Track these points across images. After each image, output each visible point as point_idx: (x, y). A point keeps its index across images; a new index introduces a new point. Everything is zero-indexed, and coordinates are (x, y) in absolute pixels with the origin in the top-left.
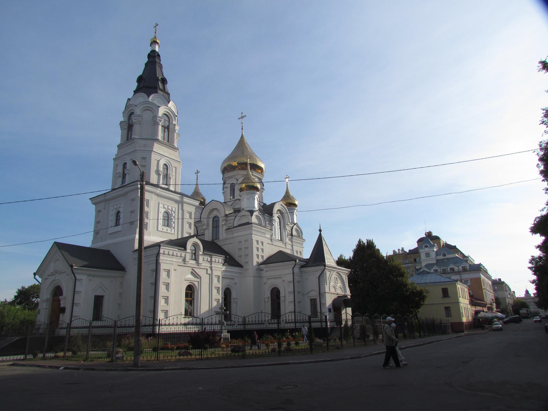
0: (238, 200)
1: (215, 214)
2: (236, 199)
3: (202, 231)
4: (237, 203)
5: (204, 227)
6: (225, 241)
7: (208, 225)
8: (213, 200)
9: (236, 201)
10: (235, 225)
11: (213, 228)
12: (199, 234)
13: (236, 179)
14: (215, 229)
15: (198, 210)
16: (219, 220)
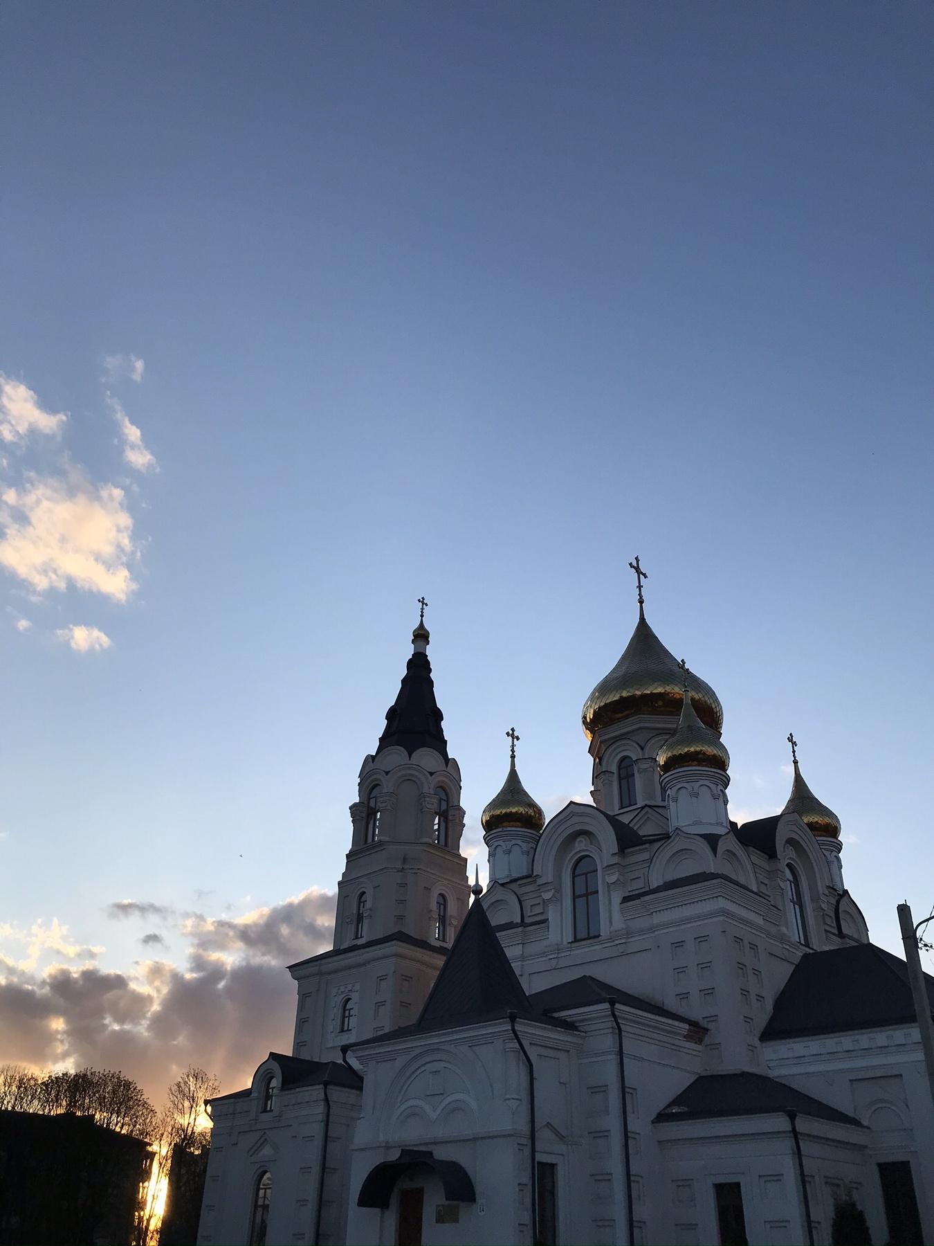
0: (647, 809)
1: (580, 851)
2: (640, 804)
3: (538, 910)
4: (646, 817)
5: (547, 896)
6: (623, 941)
7: (559, 890)
8: (571, 802)
9: (643, 812)
10: (655, 884)
11: (575, 897)
12: (527, 920)
13: (638, 744)
14: (581, 902)
15: (519, 842)
16: (597, 871)
